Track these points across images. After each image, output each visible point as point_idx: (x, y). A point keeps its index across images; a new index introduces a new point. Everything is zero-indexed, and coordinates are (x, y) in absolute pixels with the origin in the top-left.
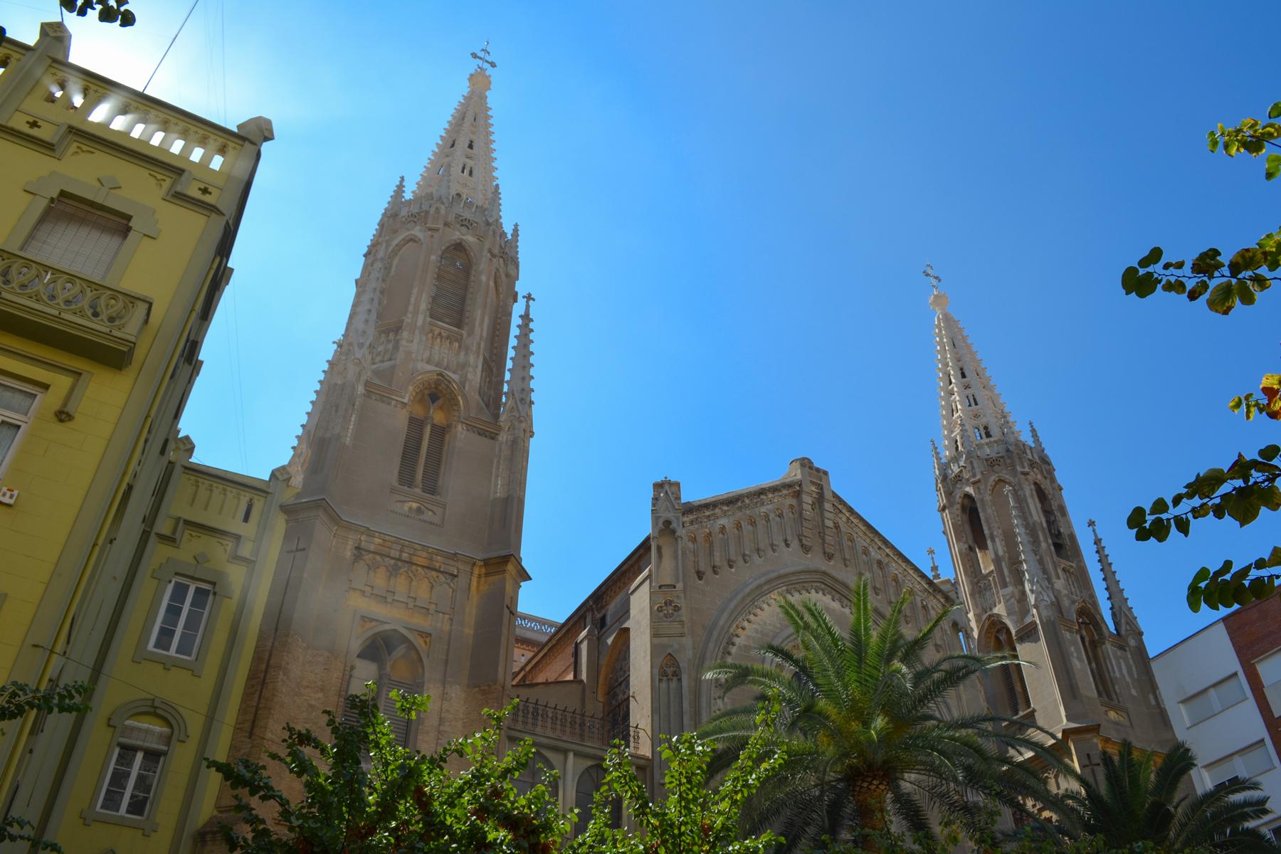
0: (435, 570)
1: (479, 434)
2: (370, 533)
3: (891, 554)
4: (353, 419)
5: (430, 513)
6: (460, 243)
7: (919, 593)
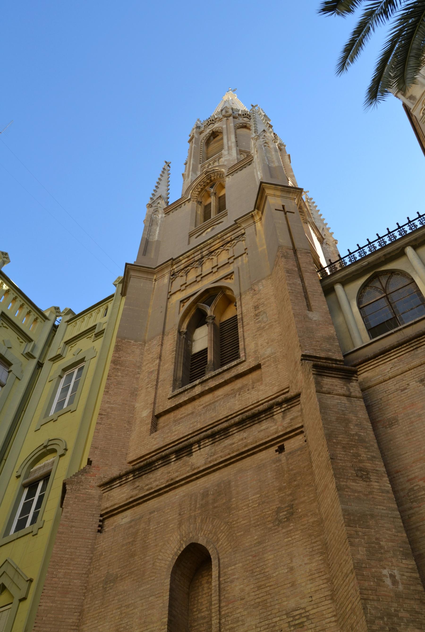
0: (228, 242)
2: (173, 261)
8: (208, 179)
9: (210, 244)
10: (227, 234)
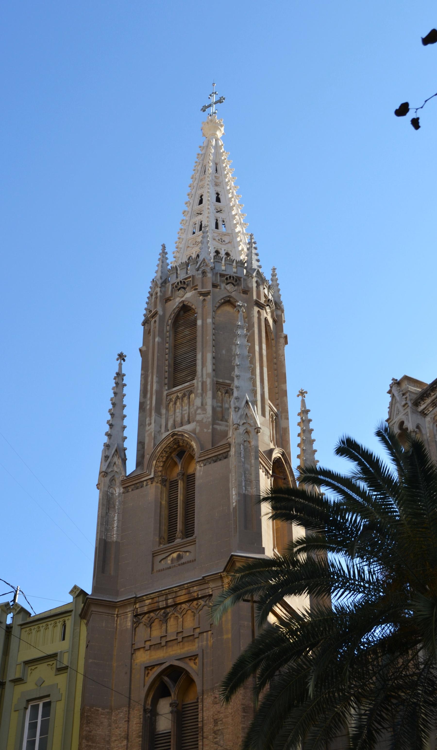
1: (215, 461)
2: (137, 600)
4: (116, 518)
5: (188, 554)
6: (184, 305)
8: (176, 444)
9: (176, 592)
10: (194, 587)
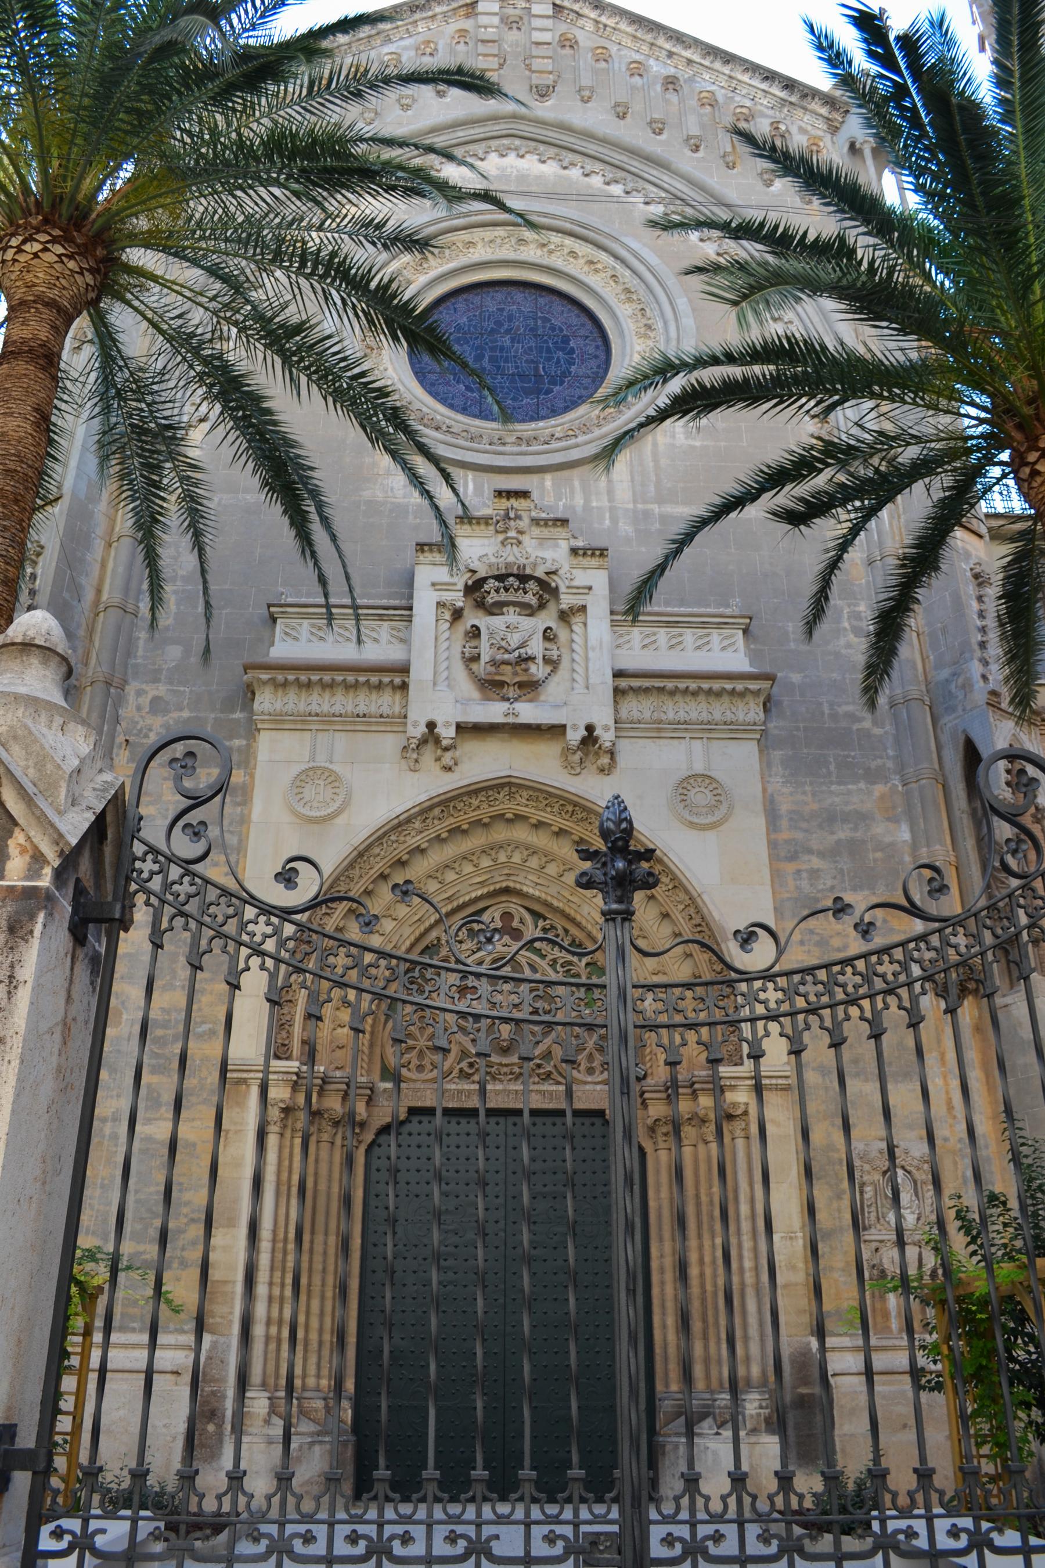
3: (696, 58)
7: (770, 112)
